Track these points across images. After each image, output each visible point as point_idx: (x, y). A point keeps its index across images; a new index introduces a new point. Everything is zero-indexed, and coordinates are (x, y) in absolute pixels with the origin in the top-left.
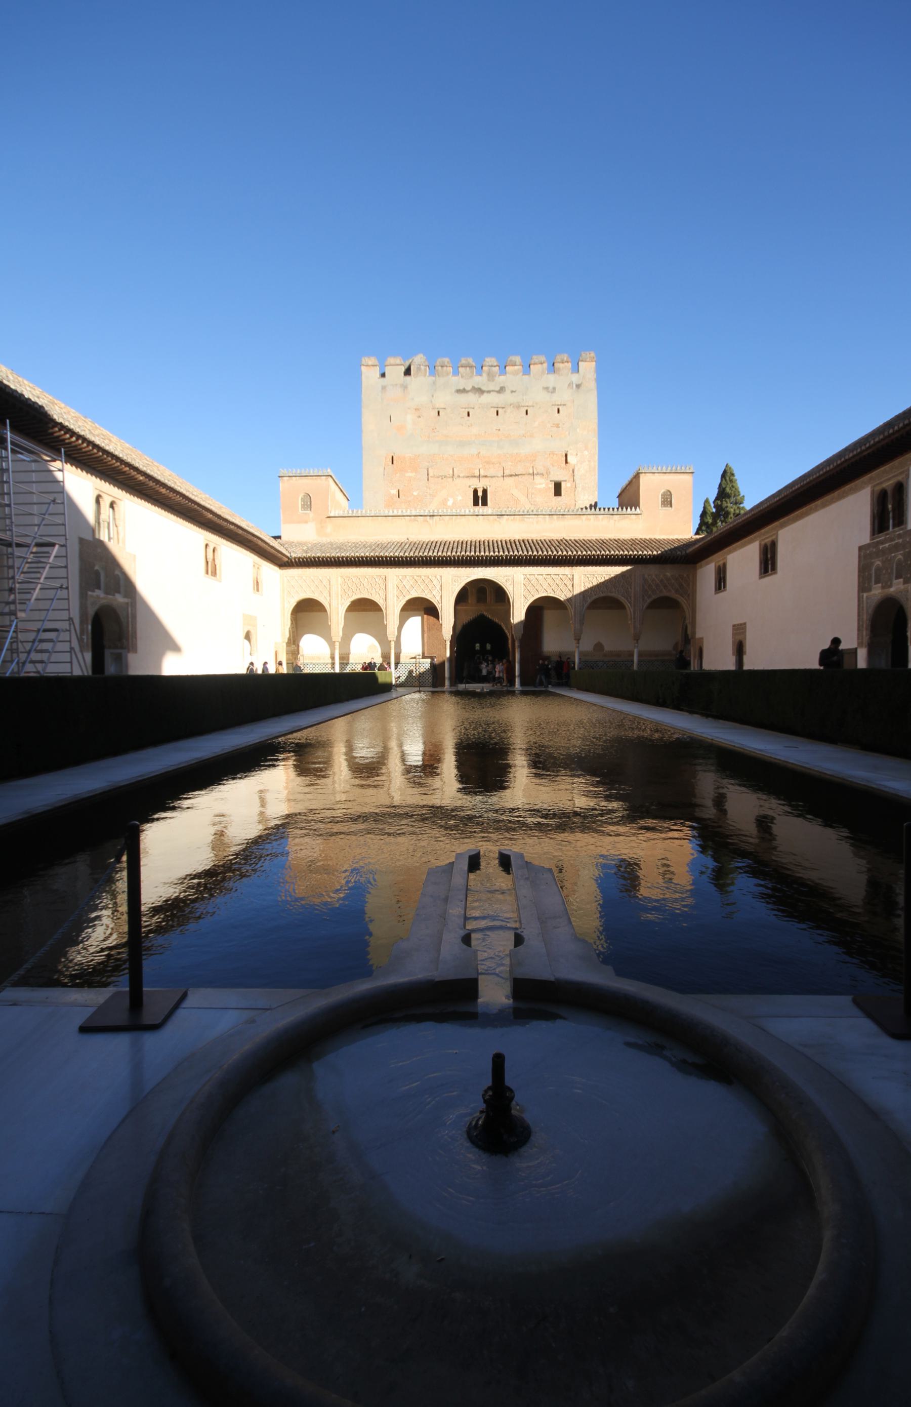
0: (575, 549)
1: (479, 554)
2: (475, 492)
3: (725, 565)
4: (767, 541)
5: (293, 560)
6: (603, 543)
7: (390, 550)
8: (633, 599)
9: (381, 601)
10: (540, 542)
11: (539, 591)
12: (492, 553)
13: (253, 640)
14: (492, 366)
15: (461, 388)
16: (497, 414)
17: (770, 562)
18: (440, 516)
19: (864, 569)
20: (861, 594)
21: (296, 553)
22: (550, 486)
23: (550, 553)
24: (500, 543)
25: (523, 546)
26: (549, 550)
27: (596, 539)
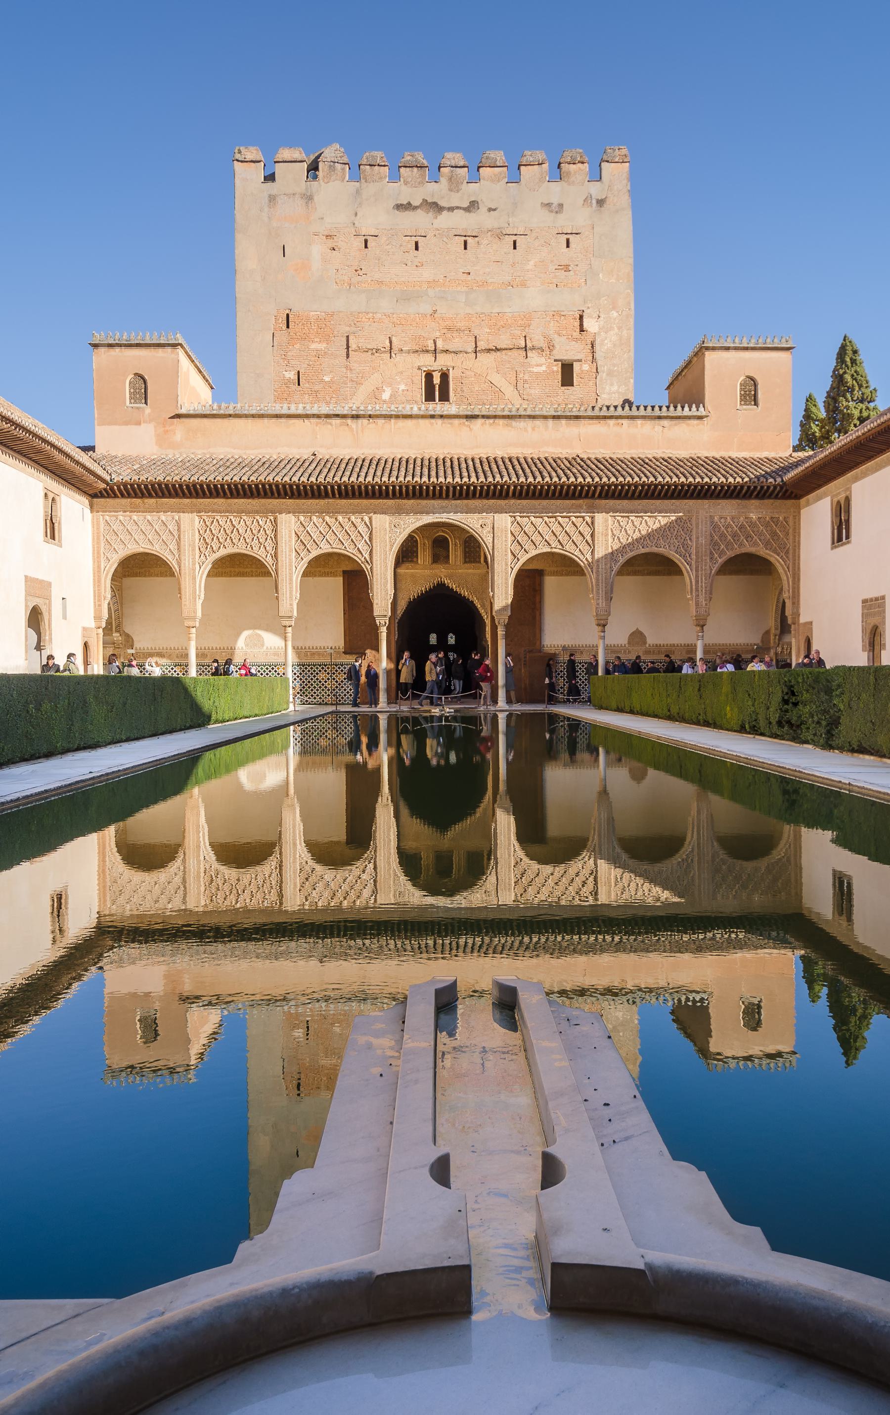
0: (597, 474)
1: (435, 480)
3: (848, 500)
7: (284, 471)
8: (694, 557)
9: (269, 558)
10: (538, 462)
11: (537, 543)
12: (457, 480)
14: (456, 167)
15: (405, 203)
16: (465, 248)
18: (370, 416)
22: (555, 369)
23: (555, 479)
24: (470, 463)
25: (510, 467)
26: (554, 474)
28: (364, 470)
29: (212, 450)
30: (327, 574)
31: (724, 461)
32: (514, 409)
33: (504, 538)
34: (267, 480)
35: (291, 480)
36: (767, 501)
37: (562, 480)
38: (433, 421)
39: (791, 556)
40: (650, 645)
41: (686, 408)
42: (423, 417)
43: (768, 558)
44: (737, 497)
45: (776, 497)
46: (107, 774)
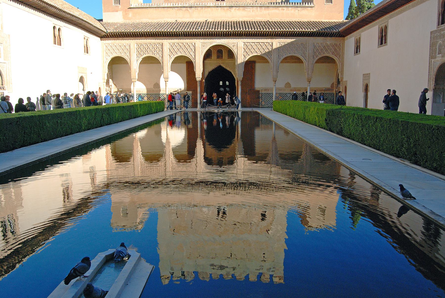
3: (360, 38)
4: (382, 25)
5: (108, 34)
6: (291, 24)
7: (165, 27)
8: (307, 57)
9: (160, 58)
11: (253, 52)
13: (85, 83)
17: (384, 38)
18: (196, 7)
19: (432, 45)
21: (111, 30)
25: (244, 25)
26: (259, 28)
27: (287, 22)
28: (193, 27)
29: (141, 20)
31: (319, 23)
32: (246, 4)
33: (241, 51)
35: (167, 31)
36: (333, 38)
37: (261, 30)
39: (341, 57)
40: (292, 88)
41: (307, 4)
42: (214, 7)
43: (333, 58)
44: (323, 36)
45: (336, 36)
46: (85, 144)
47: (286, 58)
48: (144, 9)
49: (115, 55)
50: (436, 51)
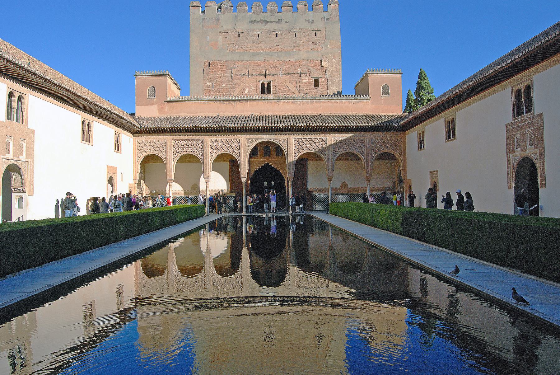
1: (265, 125)
2: (263, 84)
3: (423, 132)
4: (449, 118)
5: (142, 130)
7: (206, 122)
9: (200, 156)
11: (305, 149)
13: (114, 184)
17: (451, 132)
18: (240, 100)
19: (509, 139)
20: (509, 154)
21: (144, 125)
22: (311, 81)
26: (311, 122)
29: (179, 114)
30: (223, 161)
34: (199, 126)
37: (314, 125)
38: (264, 101)
41: (362, 96)
43: (394, 154)
45: (397, 131)
47: (341, 156)
48: (182, 102)
49: (149, 153)
50: (513, 145)
